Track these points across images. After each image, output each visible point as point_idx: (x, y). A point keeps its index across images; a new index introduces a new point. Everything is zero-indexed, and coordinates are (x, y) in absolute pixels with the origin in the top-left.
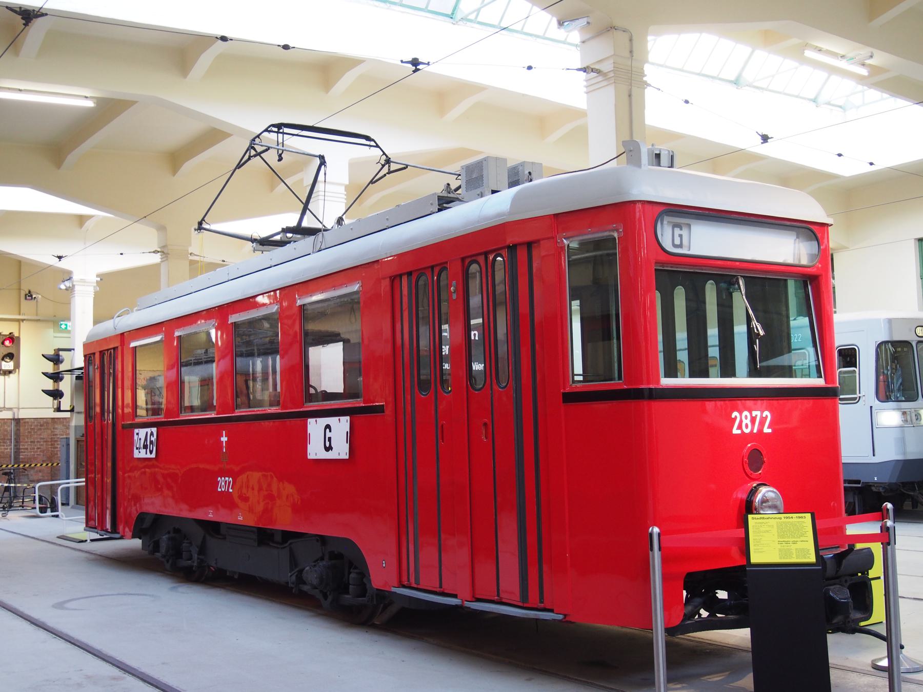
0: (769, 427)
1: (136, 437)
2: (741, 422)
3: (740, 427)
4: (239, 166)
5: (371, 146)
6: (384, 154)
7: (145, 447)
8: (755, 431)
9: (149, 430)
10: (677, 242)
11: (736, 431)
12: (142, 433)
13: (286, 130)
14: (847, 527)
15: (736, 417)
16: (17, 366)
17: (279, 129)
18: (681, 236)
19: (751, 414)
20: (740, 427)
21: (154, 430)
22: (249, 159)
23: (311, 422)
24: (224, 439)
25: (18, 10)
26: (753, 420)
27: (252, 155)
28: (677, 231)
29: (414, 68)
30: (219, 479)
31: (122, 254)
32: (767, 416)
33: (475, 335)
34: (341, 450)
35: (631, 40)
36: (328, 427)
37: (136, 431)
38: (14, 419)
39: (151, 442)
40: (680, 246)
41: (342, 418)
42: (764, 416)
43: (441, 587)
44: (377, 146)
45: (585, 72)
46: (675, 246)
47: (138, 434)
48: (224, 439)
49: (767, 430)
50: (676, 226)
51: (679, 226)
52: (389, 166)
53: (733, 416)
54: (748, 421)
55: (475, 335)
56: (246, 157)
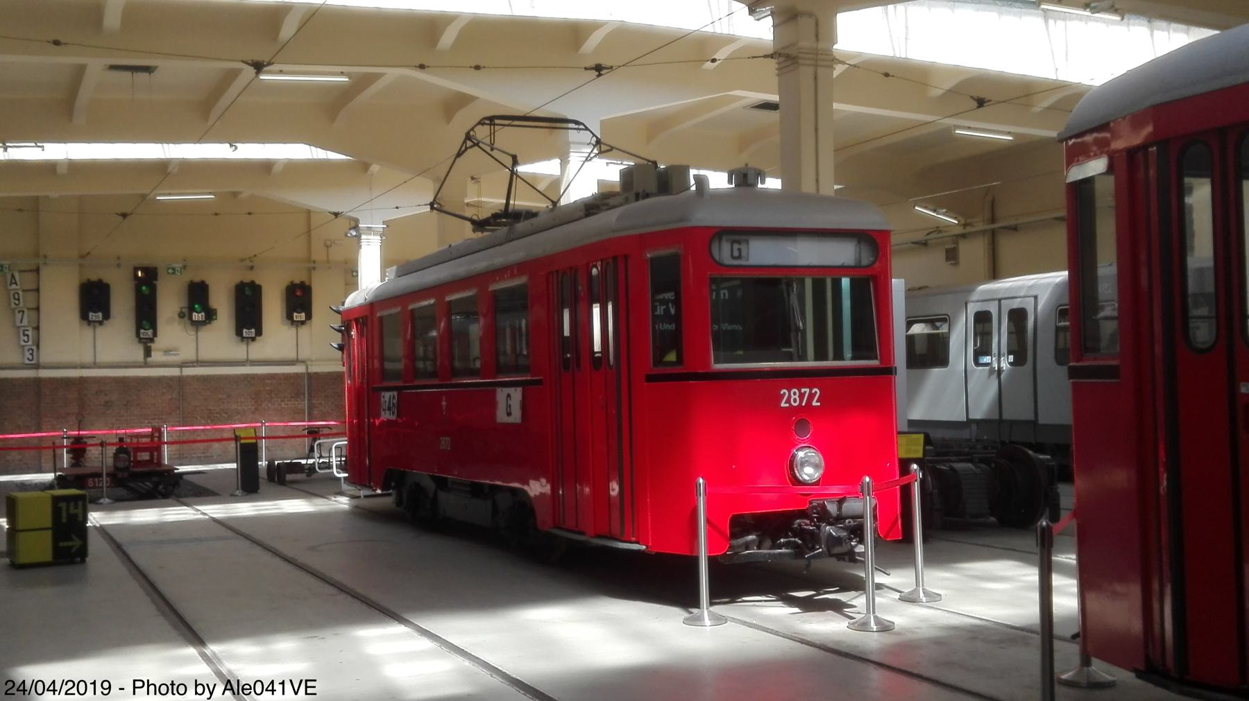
0: (817, 402)
1: (382, 399)
2: (790, 396)
3: (788, 401)
4: (459, 155)
5: (581, 129)
6: (594, 135)
7: (389, 409)
8: (803, 404)
9: (391, 393)
10: (736, 254)
11: (783, 405)
12: (386, 396)
13: (497, 121)
14: (1059, 490)
15: (785, 393)
16: (309, 317)
17: (491, 122)
18: (739, 250)
19: (800, 391)
20: (788, 401)
21: (396, 393)
22: (466, 149)
23: (499, 390)
24: (444, 403)
25: (250, 62)
26: (802, 396)
27: (472, 144)
28: (736, 246)
29: (597, 73)
30: (441, 438)
31: (397, 208)
32: (816, 392)
33: (724, 294)
34: (516, 417)
35: (817, 24)
36: (509, 396)
37: (383, 394)
38: (309, 374)
39: (393, 404)
40: (739, 257)
41: (517, 389)
42: (813, 391)
43: (577, 527)
44: (587, 129)
45: (772, 58)
46: (733, 257)
47: (384, 397)
48: (444, 403)
49: (815, 403)
50: (733, 242)
51: (739, 242)
52: (600, 147)
53: (782, 393)
54: (797, 397)
55: (724, 294)
56: (463, 148)
